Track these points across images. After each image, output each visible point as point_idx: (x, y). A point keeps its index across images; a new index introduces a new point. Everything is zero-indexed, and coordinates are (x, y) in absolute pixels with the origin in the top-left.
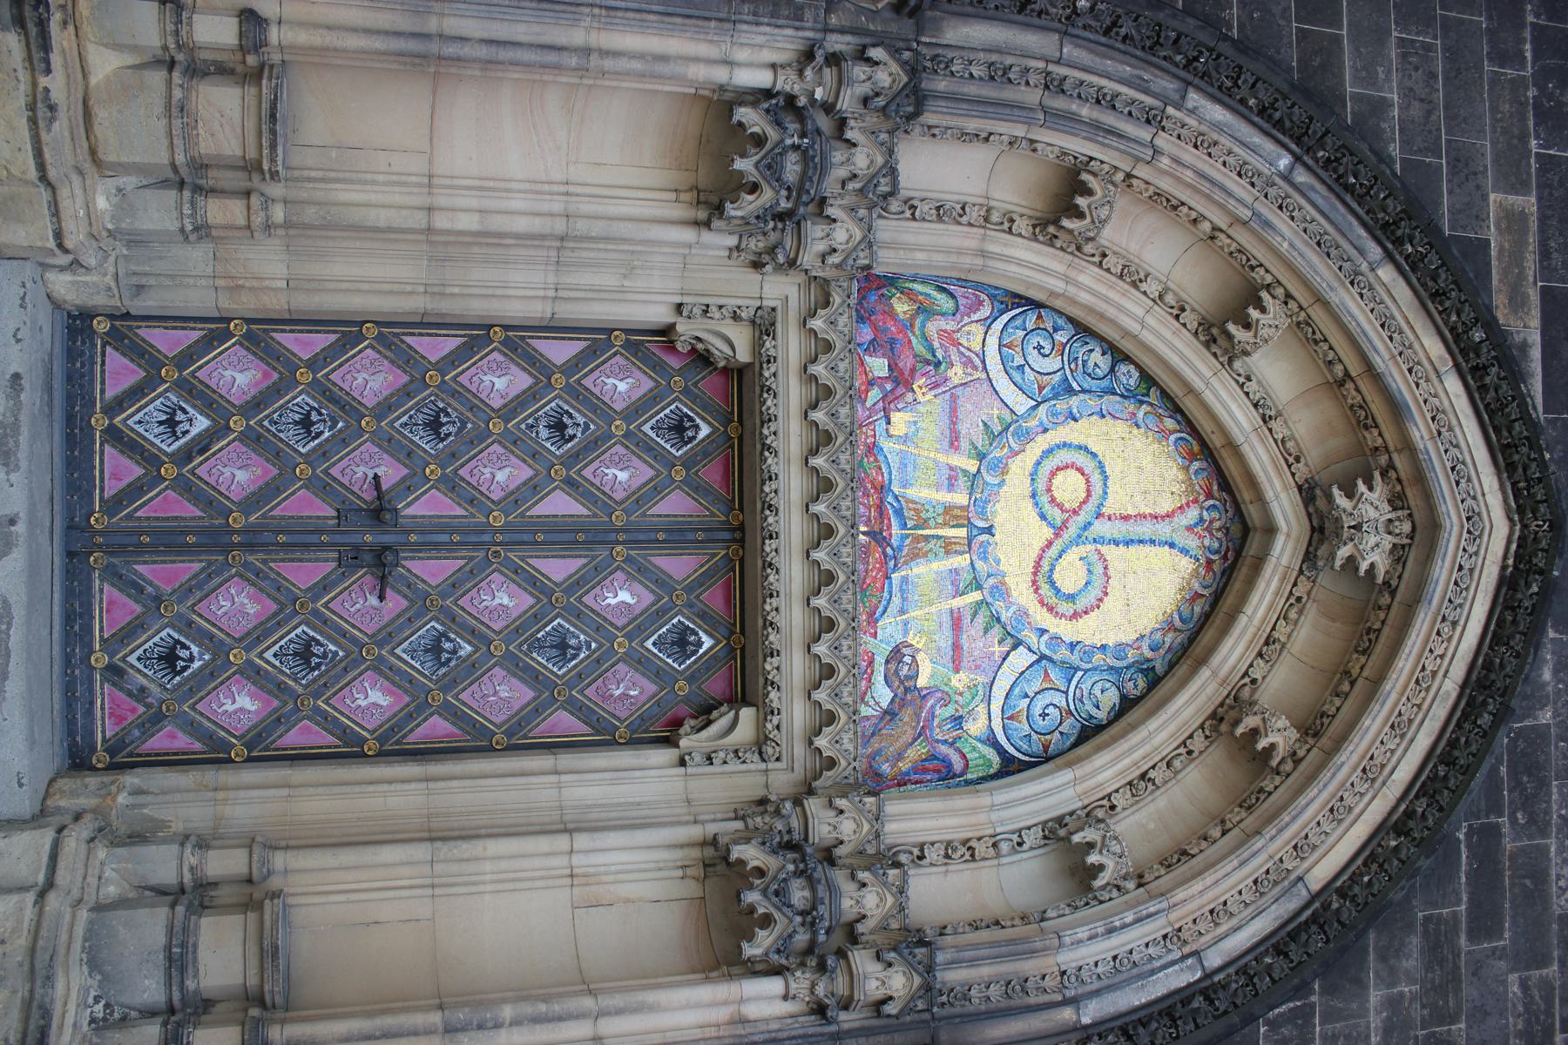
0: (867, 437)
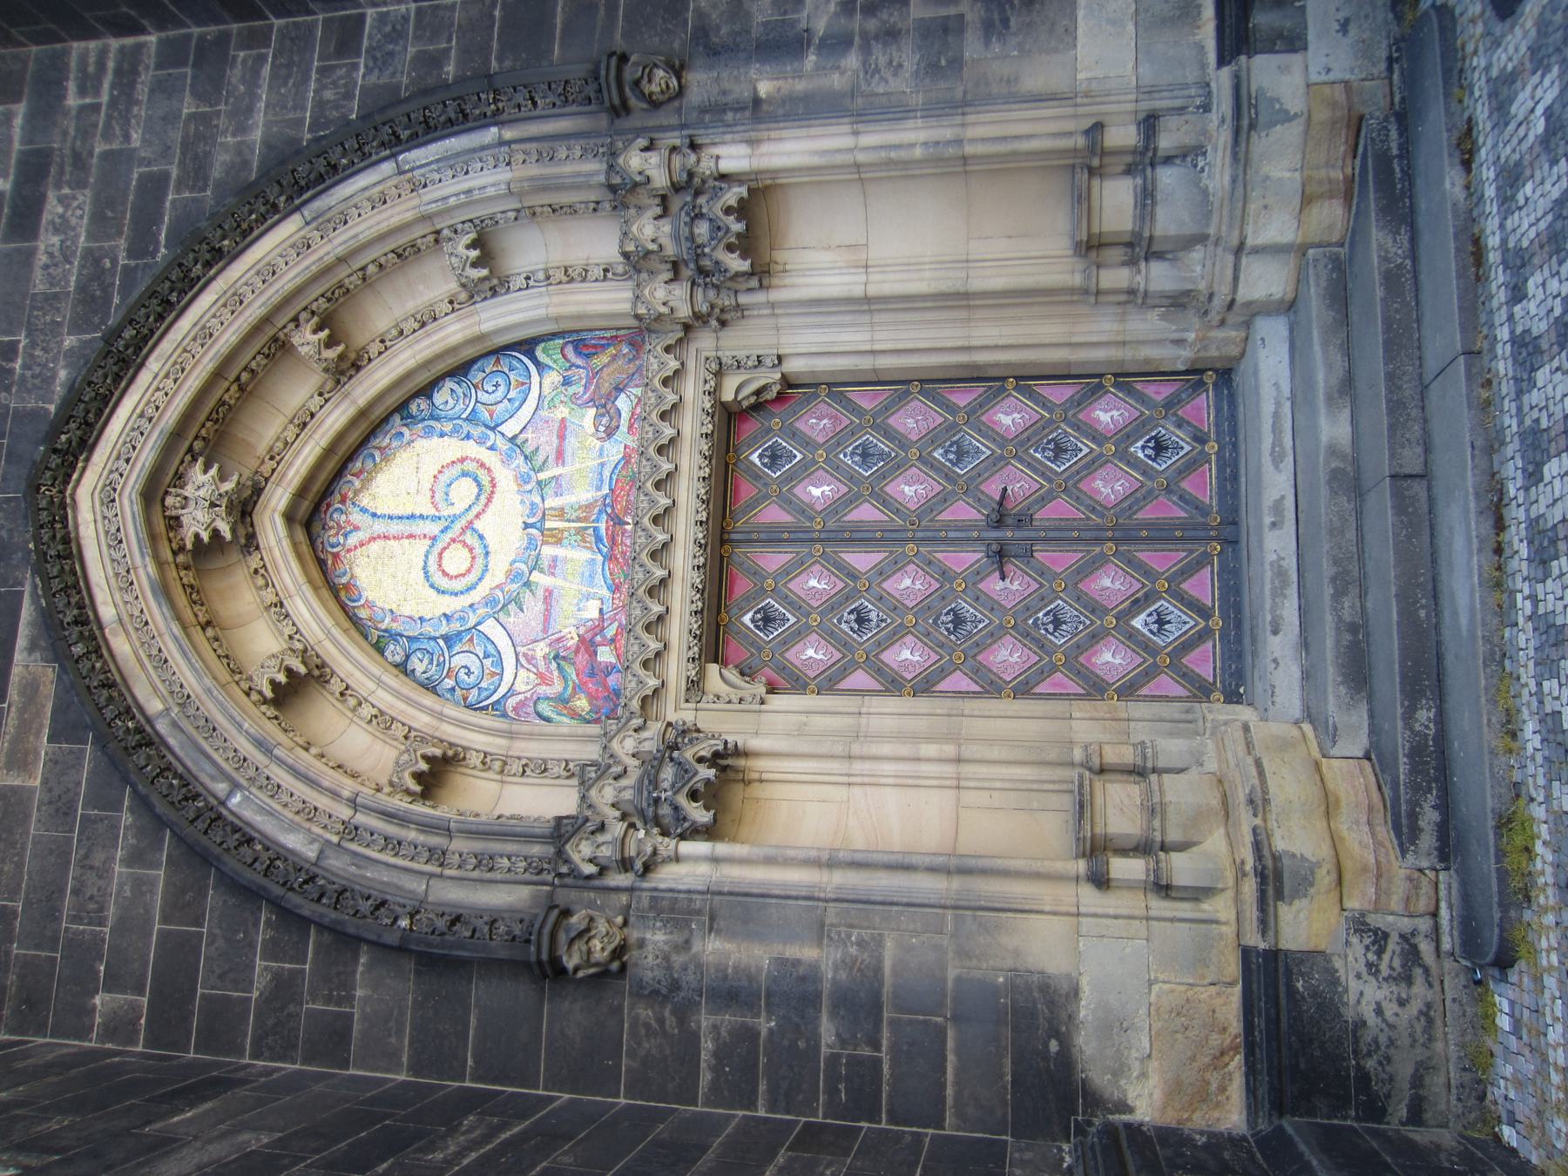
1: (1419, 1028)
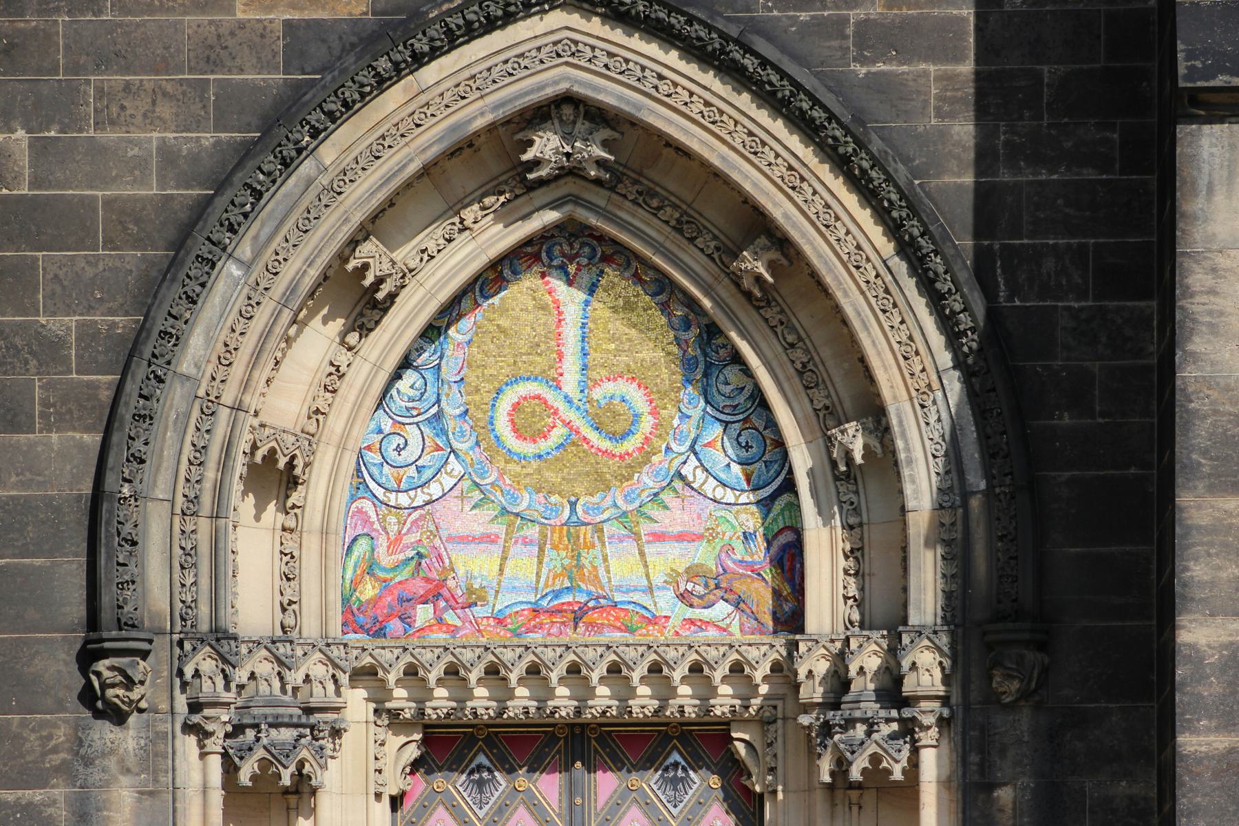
0: (489, 625)
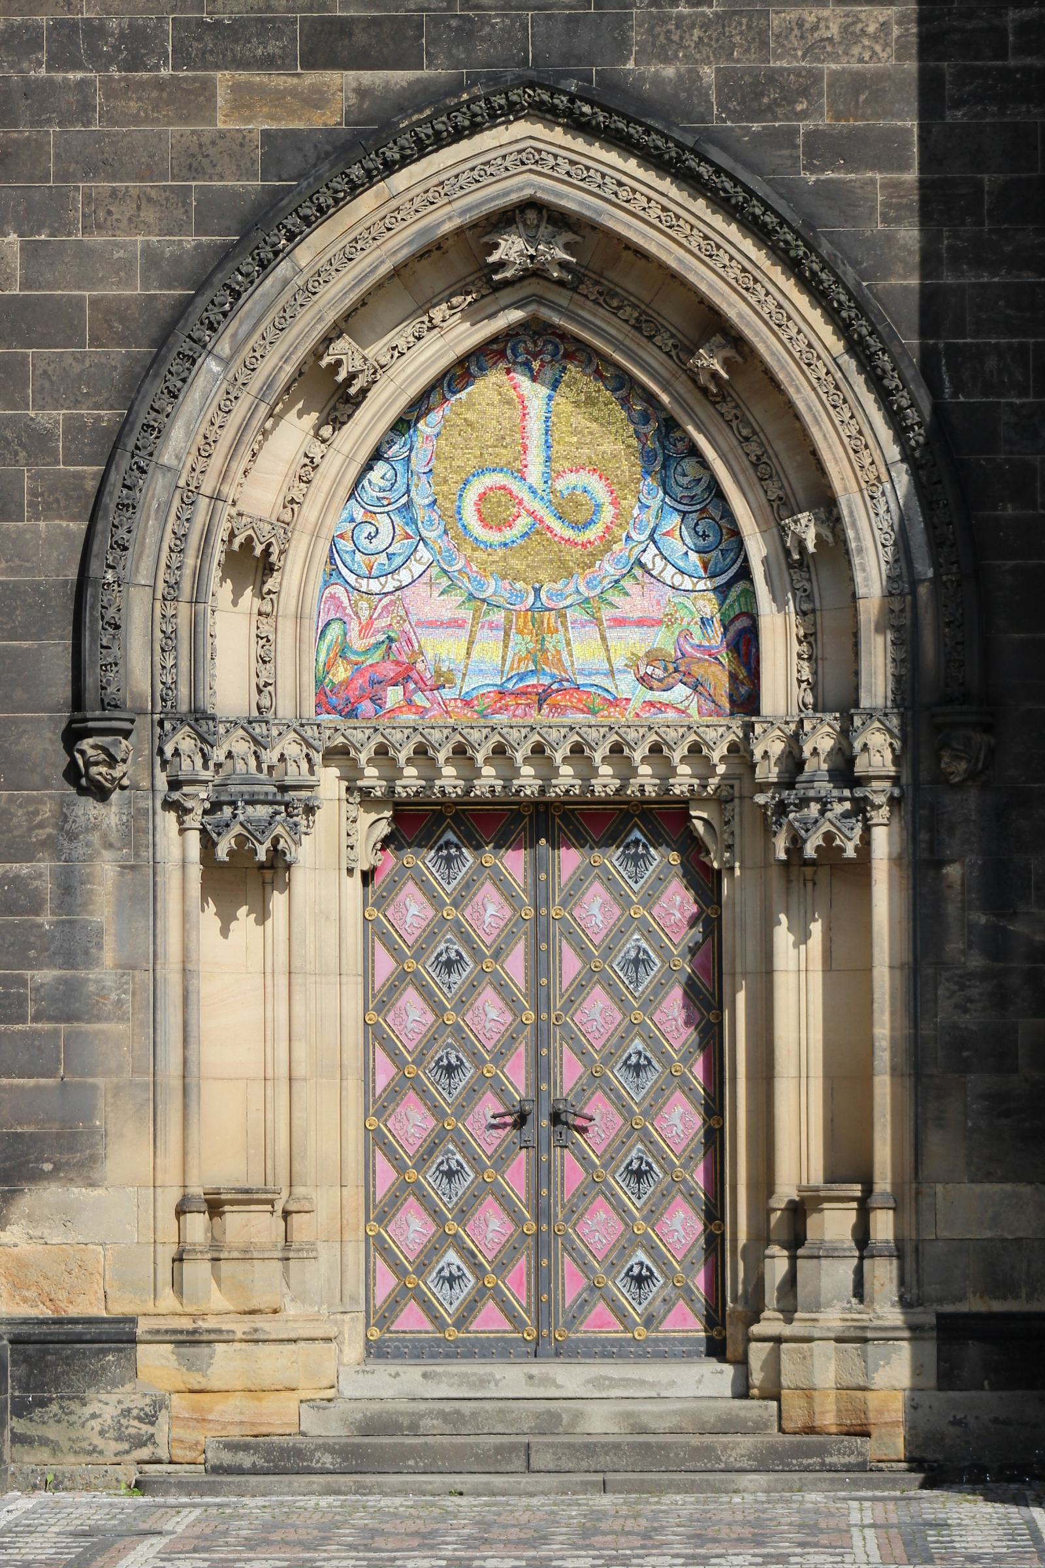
0: (456, 707)
1: (85, 1445)
